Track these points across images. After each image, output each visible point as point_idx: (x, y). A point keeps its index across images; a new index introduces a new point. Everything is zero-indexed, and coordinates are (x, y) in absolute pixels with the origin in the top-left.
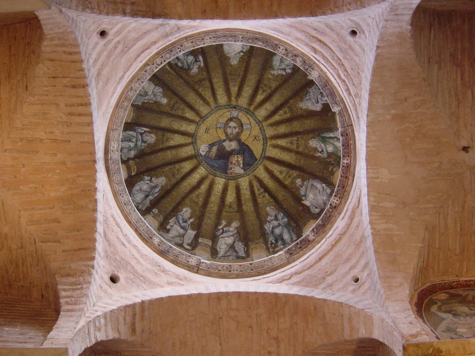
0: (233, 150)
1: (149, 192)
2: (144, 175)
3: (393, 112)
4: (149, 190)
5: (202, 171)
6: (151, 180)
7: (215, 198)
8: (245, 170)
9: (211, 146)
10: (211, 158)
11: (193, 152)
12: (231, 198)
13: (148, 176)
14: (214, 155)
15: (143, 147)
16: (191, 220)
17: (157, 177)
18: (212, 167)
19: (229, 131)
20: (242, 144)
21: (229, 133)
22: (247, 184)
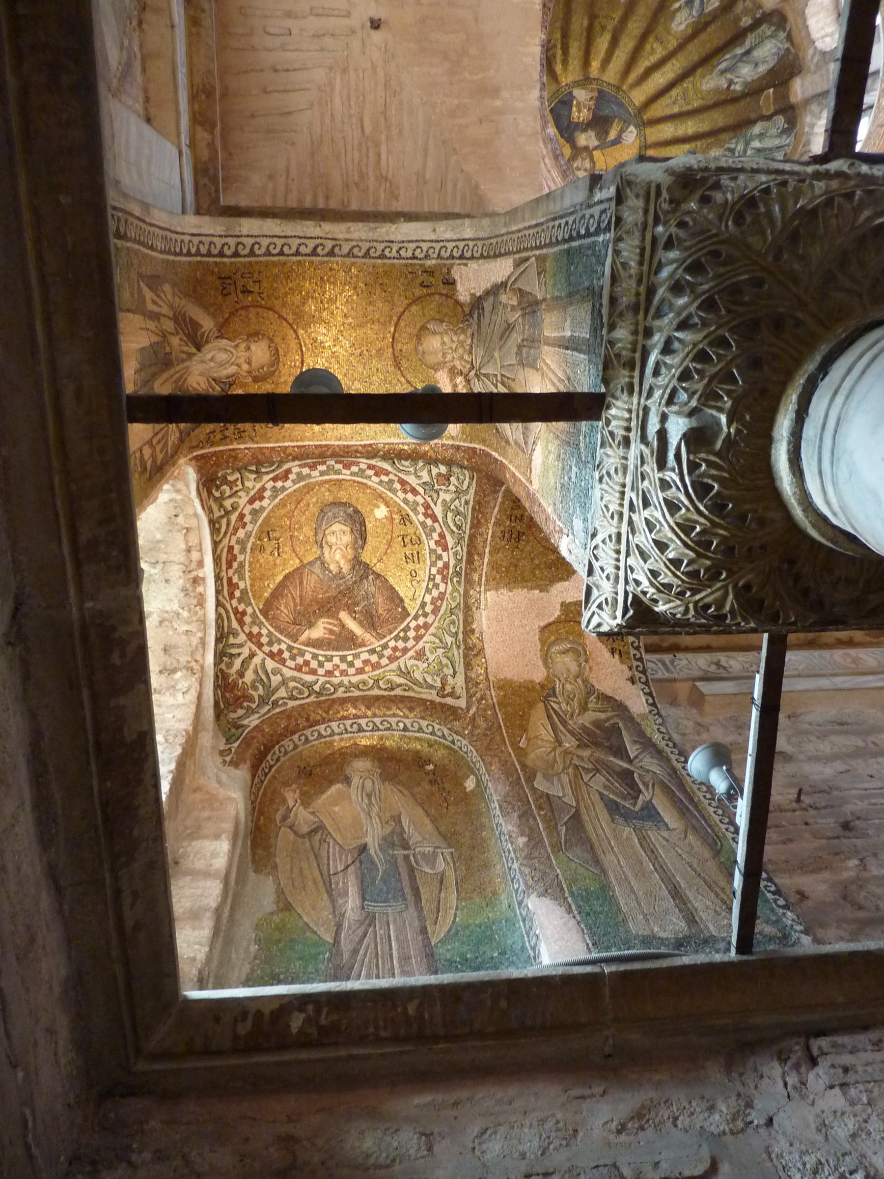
0: (584, 130)
1: (740, 60)
2: (743, 91)
3: (498, 103)
4: (740, 64)
5: (638, 96)
6: (731, 82)
7: (626, 45)
8: (571, 93)
9: (617, 141)
10: (620, 118)
11: (648, 131)
12: (602, 43)
13: (734, 91)
14: (615, 125)
15: (734, 141)
16: (677, 5)
17: (717, 91)
18: (621, 105)
19: (587, 164)
20: (571, 140)
21: (587, 161)
22: (571, 68)
